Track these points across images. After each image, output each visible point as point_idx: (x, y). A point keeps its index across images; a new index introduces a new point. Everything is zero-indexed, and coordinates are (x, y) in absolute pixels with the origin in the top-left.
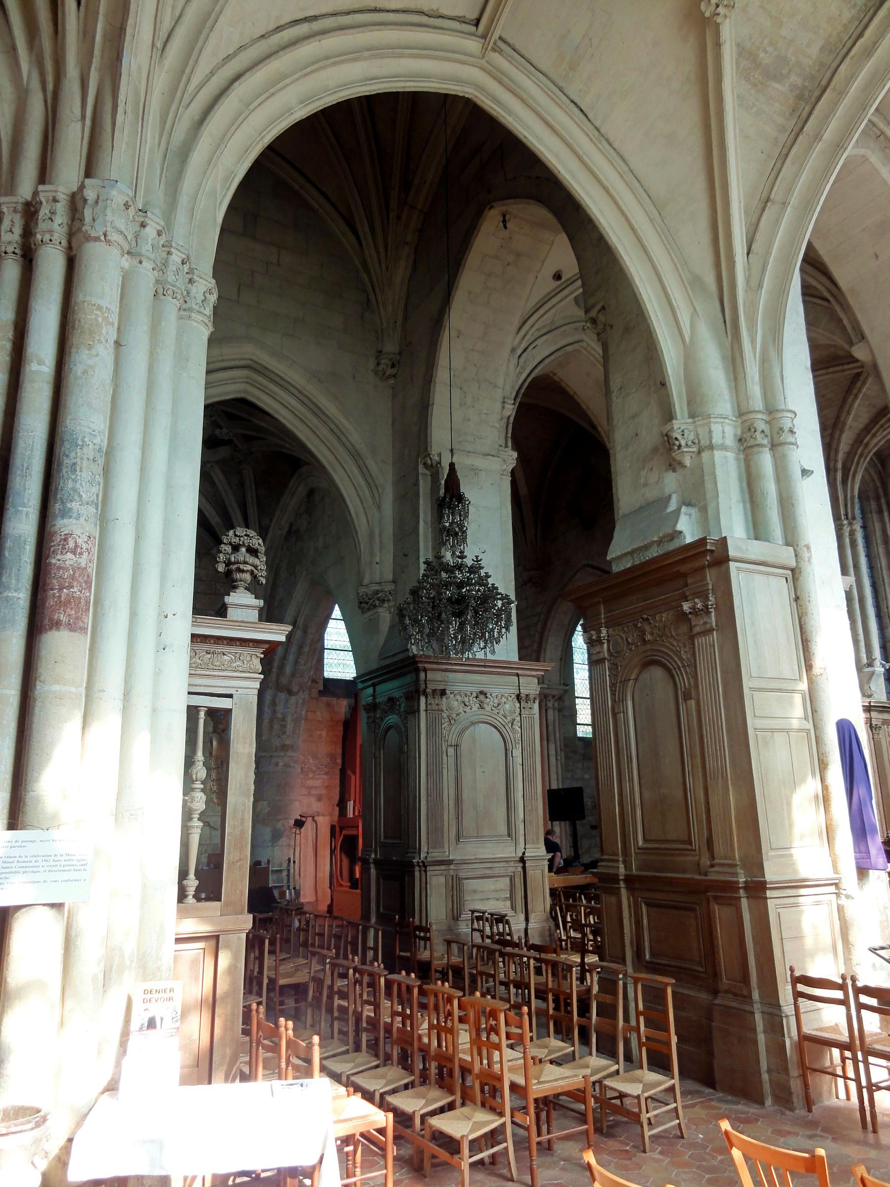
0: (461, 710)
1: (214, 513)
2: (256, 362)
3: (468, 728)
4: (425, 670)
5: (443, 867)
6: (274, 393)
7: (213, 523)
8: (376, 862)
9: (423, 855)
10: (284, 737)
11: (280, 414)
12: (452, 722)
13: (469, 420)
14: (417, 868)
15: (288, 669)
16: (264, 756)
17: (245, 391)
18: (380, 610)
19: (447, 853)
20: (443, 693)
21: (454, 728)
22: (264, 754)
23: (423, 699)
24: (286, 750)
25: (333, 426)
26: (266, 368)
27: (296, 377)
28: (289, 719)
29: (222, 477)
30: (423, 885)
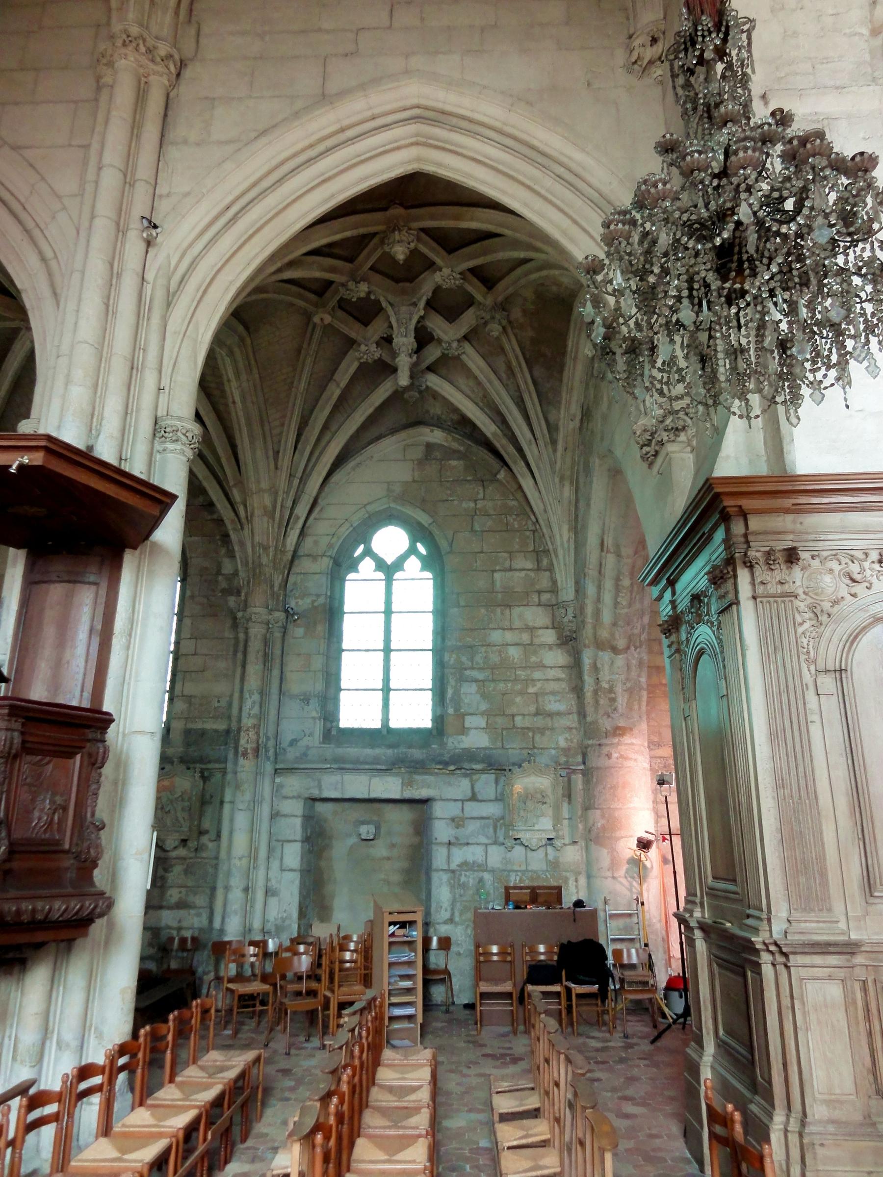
0: (843, 591)
1: (488, 421)
2: (426, 108)
3: (864, 629)
4: (744, 515)
5: (833, 960)
6: (456, 145)
7: (489, 435)
8: (703, 927)
9: (778, 928)
10: (615, 715)
11: (477, 179)
12: (824, 618)
13: (795, 34)
14: (765, 958)
15: (607, 617)
16: (592, 745)
17: (419, 159)
18: (670, 448)
19: (842, 925)
20: (792, 556)
21: (827, 634)
22: (590, 742)
23: (743, 576)
24: (622, 735)
25: (561, 170)
26: (443, 112)
27: (489, 110)
28: (619, 689)
29: (482, 363)
30: (786, 1002)
